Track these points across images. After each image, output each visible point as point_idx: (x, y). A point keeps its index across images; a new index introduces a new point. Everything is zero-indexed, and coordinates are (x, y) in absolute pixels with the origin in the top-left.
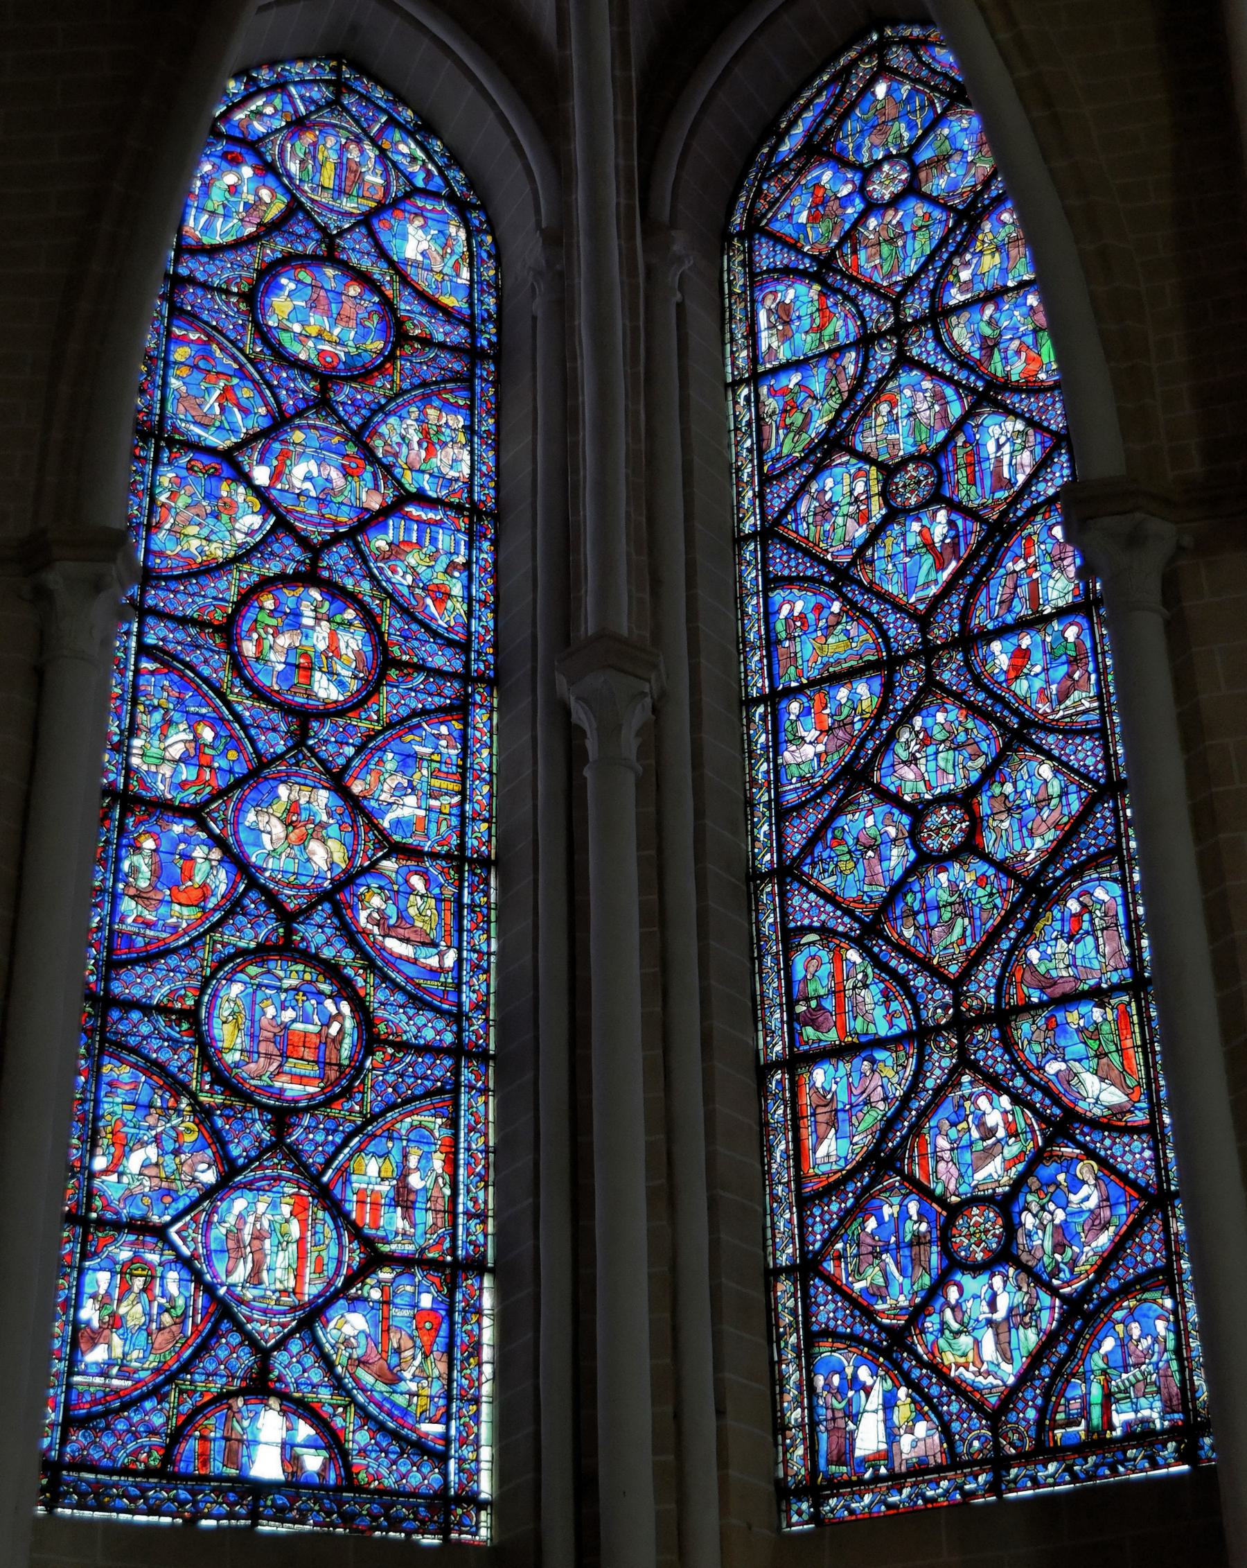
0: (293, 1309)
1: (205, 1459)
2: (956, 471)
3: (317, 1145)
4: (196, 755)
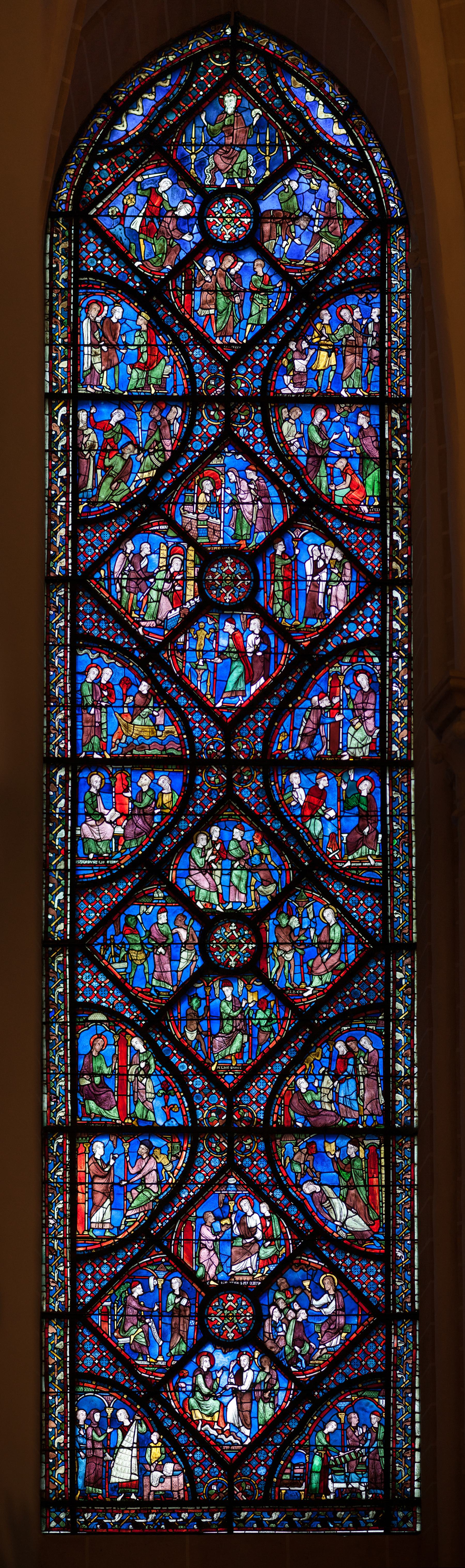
2: (273, 582)
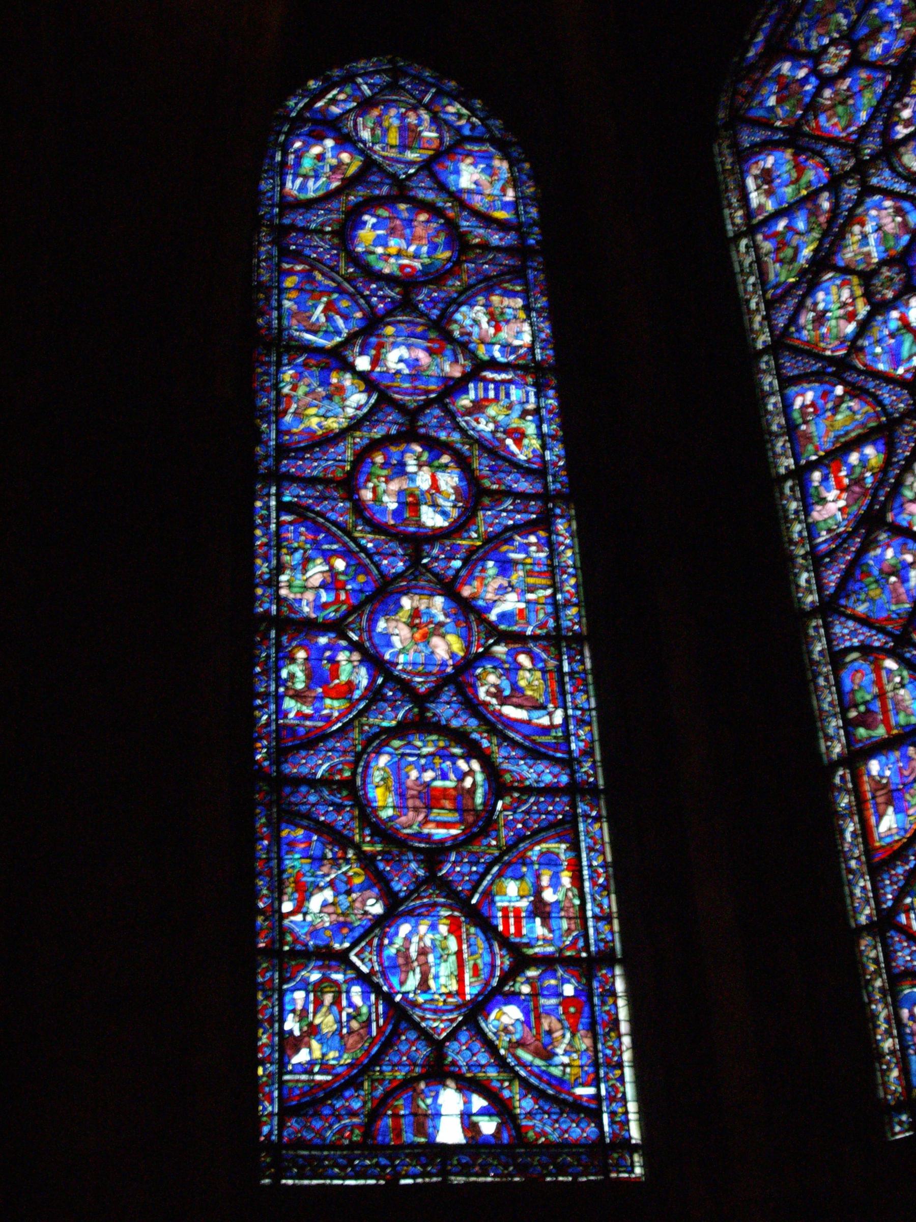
0: (458, 1007)
1: (398, 1131)
3: (463, 875)
4: (332, 583)
